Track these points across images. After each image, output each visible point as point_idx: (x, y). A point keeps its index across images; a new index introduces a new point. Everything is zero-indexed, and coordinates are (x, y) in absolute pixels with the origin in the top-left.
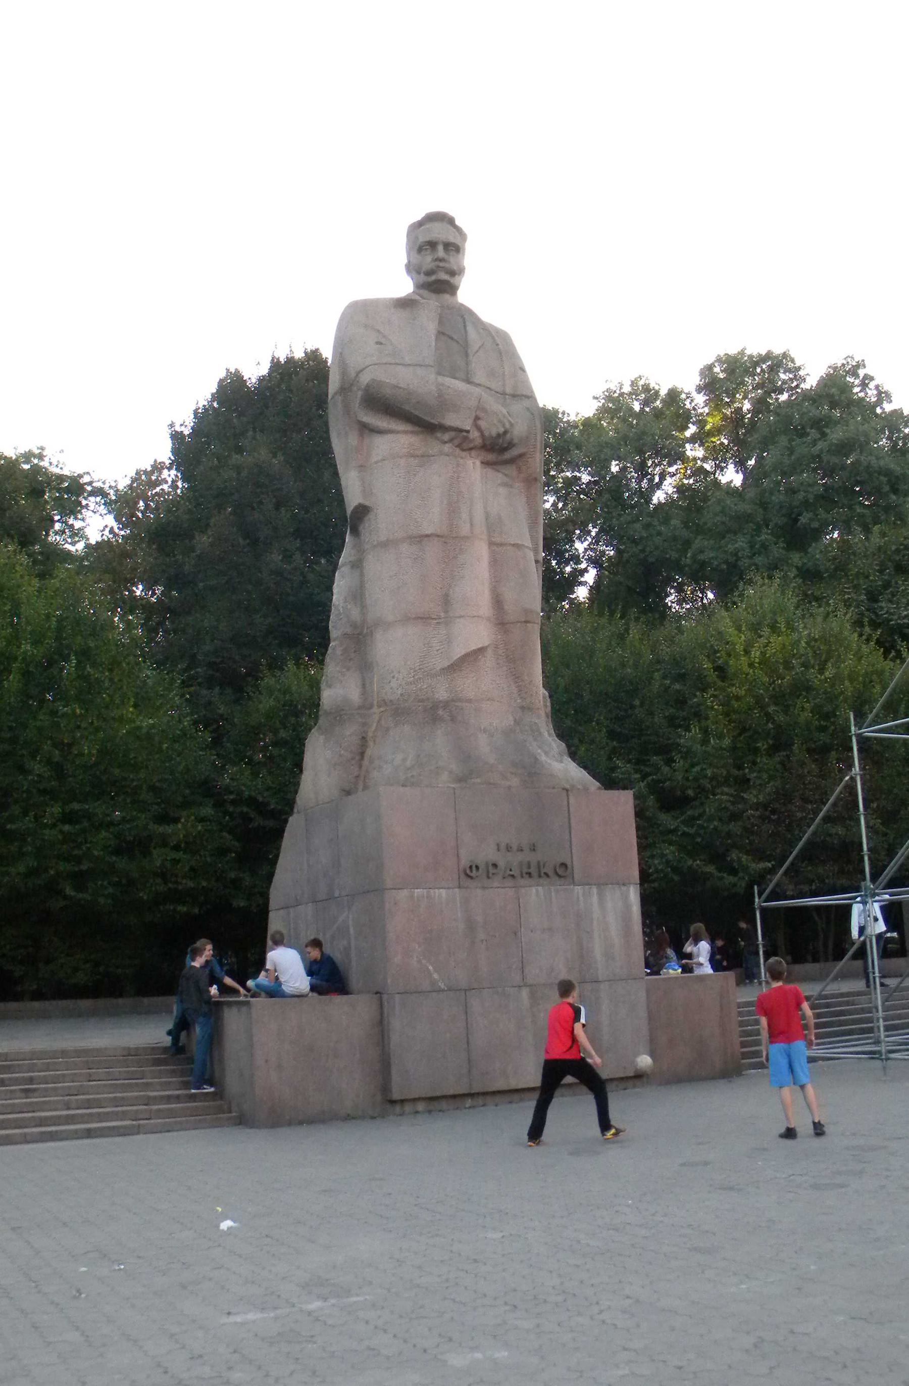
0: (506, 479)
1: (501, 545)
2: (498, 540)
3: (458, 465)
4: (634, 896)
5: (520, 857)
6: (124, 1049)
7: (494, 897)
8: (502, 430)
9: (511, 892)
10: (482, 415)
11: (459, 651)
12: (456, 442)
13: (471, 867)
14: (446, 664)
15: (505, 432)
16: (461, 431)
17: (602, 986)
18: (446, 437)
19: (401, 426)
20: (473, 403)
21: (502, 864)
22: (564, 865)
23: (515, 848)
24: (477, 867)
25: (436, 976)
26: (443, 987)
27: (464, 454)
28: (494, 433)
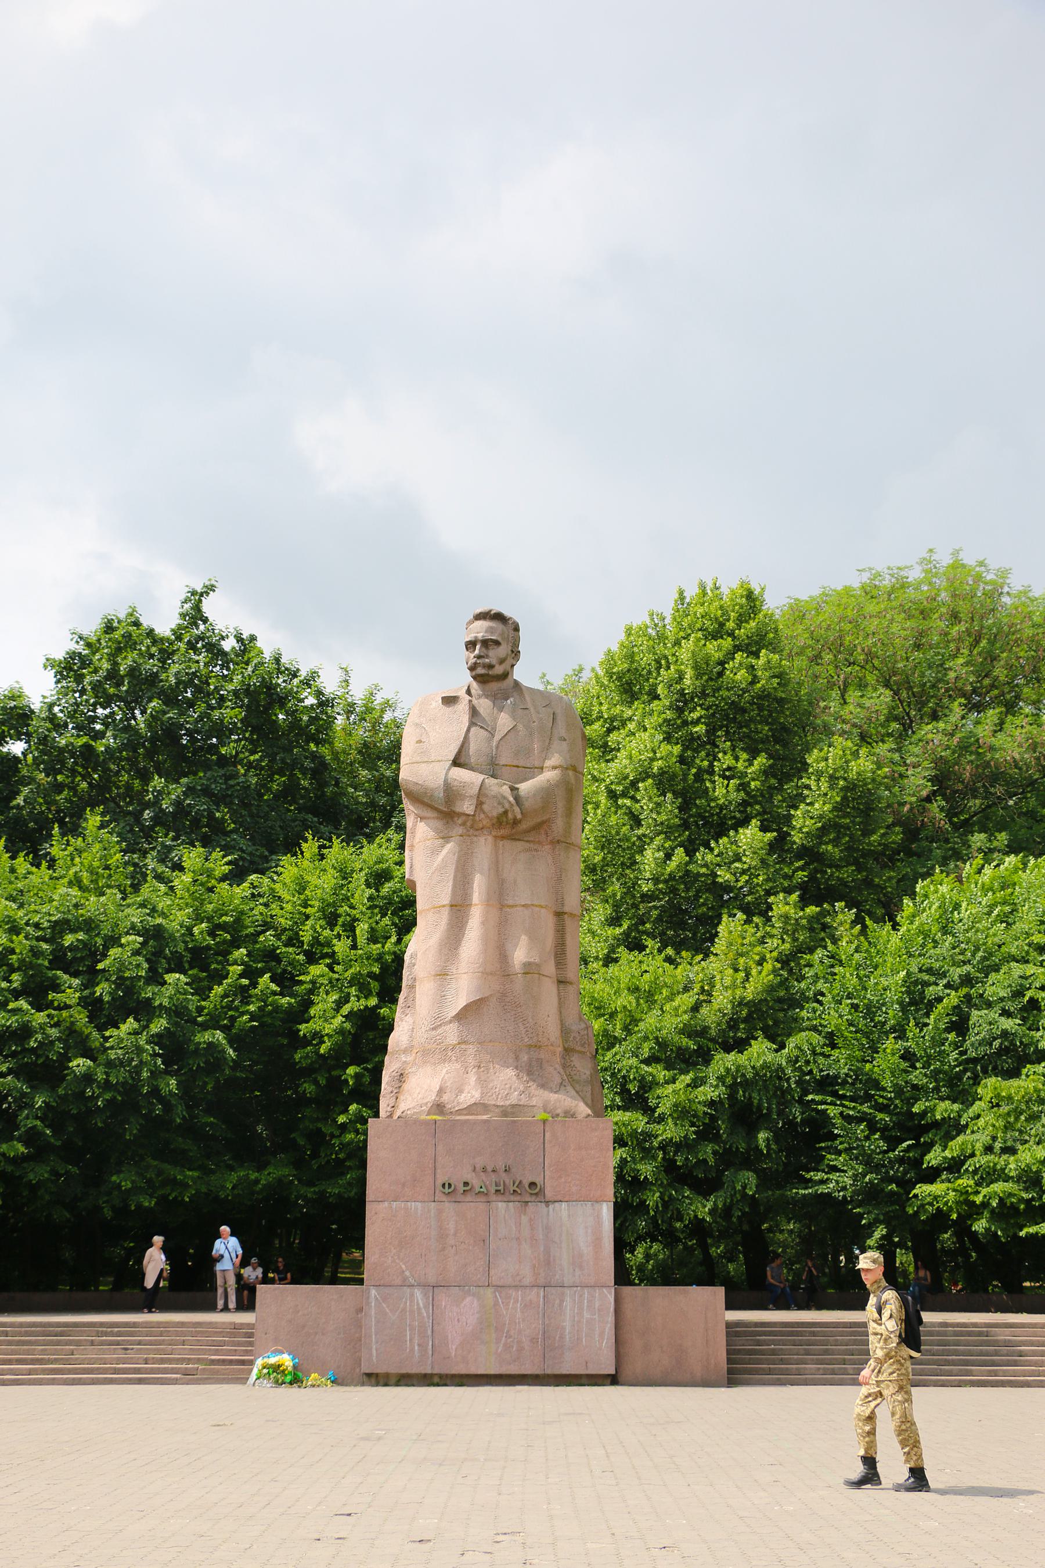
0: (527, 845)
1: (512, 906)
2: (510, 902)
3: (472, 843)
4: (606, 1212)
5: (494, 1177)
6: (231, 1323)
7: (473, 1208)
8: (501, 810)
9: (482, 1206)
10: (484, 799)
11: (462, 1003)
12: (469, 824)
13: (444, 1185)
14: (454, 1013)
15: (506, 812)
16: (469, 815)
17: (567, 1291)
18: (460, 821)
19: (429, 813)
20: (475, 790)
21: (475, 1182)
22: (533, 1184)
23: (489, 1169)
24: (450, 1185)
25: (407, 1273)
26: (412, 1281)
27: (477, 833)
28: (495, 814)
